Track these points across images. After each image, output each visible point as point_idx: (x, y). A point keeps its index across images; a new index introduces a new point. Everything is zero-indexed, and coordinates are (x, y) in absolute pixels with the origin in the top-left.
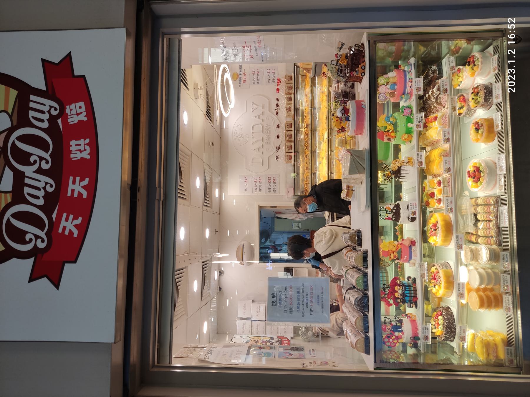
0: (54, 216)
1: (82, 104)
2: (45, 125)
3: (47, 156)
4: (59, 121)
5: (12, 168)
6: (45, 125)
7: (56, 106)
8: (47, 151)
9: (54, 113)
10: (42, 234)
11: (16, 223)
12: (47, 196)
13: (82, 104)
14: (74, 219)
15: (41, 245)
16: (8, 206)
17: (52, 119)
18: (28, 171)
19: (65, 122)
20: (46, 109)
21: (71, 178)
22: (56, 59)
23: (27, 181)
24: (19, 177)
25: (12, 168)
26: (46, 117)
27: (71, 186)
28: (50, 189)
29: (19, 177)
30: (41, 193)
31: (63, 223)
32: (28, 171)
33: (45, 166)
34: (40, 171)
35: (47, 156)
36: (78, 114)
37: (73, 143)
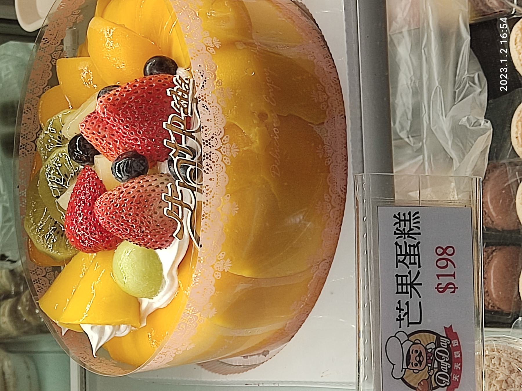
0: (451, 375)
1: (457, 340)
2: (446, 347)
3: (447, 356)
4: (450, 346)
5: (437, 361)
6: (446, 347)
7: (449, 341)
8: (447, 355)
9: (449, 343)
10: (448, 381)
11: (439, 377)
12: (448, 368)
13: (457, 340)
14: (457, 376)
15: (448, 384)
16: (437, 372)
17: (448, 345)
18: (442, 361)
19: (452, 346)
20: (446, 342)
21: (455, 364)
22: (448, 326)
23: (442, 364)
24: (439, 363)
25: (437, 361)
26: (446, 344)
27: (455, 366)
28: (449, 367)
29: (439, 363)
30: (447, 368)
31: (454, 377)
32: (442, 361)
33: (447, 360)
34: (445, 361)
35: (447, 356)
36: (456, 343)
37: (455, 352)
